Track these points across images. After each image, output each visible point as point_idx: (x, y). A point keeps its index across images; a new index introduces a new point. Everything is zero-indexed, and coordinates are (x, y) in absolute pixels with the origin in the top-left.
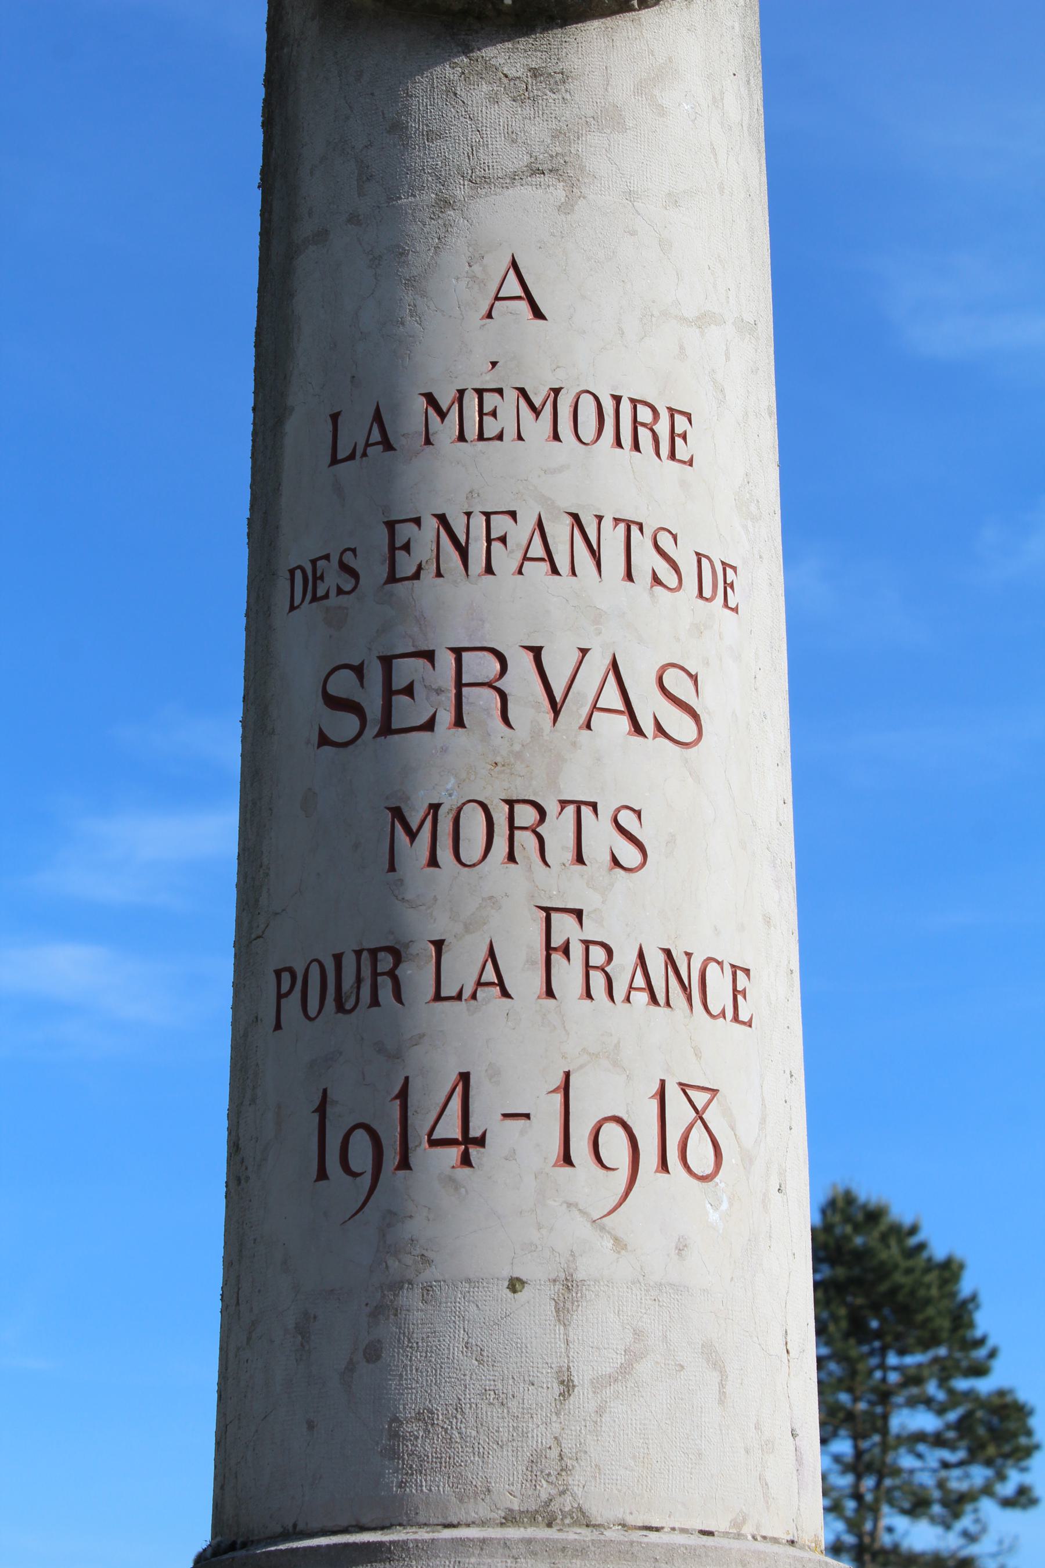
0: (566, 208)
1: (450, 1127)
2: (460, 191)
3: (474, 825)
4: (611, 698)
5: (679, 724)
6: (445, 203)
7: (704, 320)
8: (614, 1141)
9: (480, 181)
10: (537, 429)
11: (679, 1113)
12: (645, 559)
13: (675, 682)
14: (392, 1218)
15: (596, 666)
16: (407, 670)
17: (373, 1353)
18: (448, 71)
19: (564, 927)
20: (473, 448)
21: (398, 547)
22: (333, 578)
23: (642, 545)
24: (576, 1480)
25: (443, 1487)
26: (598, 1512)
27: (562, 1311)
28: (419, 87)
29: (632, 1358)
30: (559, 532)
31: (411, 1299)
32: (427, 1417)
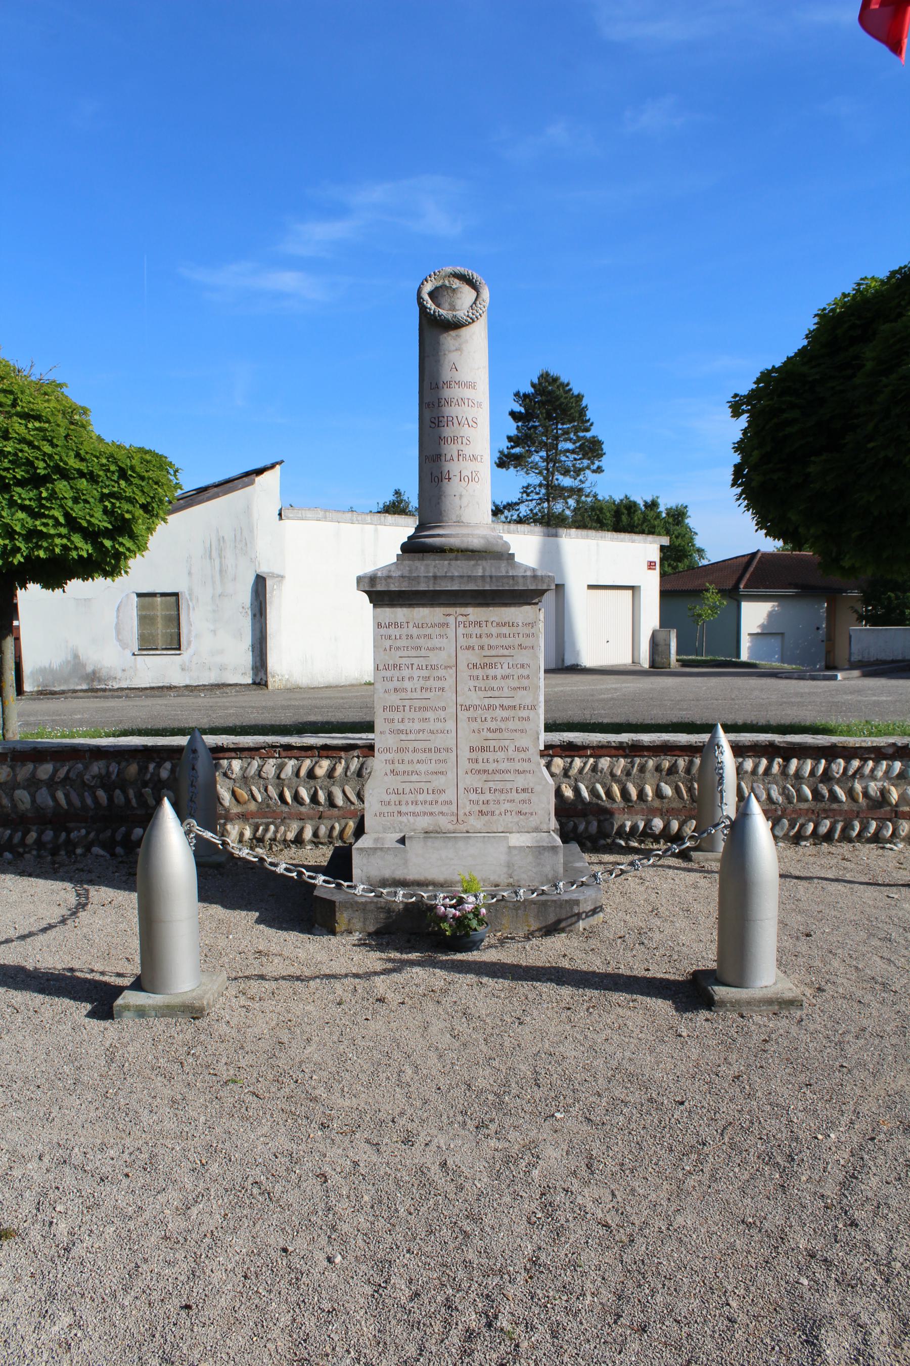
0: (461, 355)
1: (447, 477)
2: (447, 353)
3: (449, 439)
4: (466, 422)
5: (475, 425)
6: (445, 354)
7: (478, 369)
8: (466, 478)
9: (449, 351)
10: (457, 386)
11: (474, 474)
12: (471, 403)
13: (474, 420)
14: (440, 488)
15: (464, 418)
16: (441, 419)
17: (439, 503)
18: (445, 335)
19: (460, 452)
20: (448, 389)
21: (439, 402)
22: (431, 406)
23: (470, 401)
24: (462, 518)
25: (447, 519)
26: (465, 521)
27: (460, 499)
28: (441, 337)
29: (468, 504)
30: (460, 401)
31: (443, 497)
32: (445, 511)
